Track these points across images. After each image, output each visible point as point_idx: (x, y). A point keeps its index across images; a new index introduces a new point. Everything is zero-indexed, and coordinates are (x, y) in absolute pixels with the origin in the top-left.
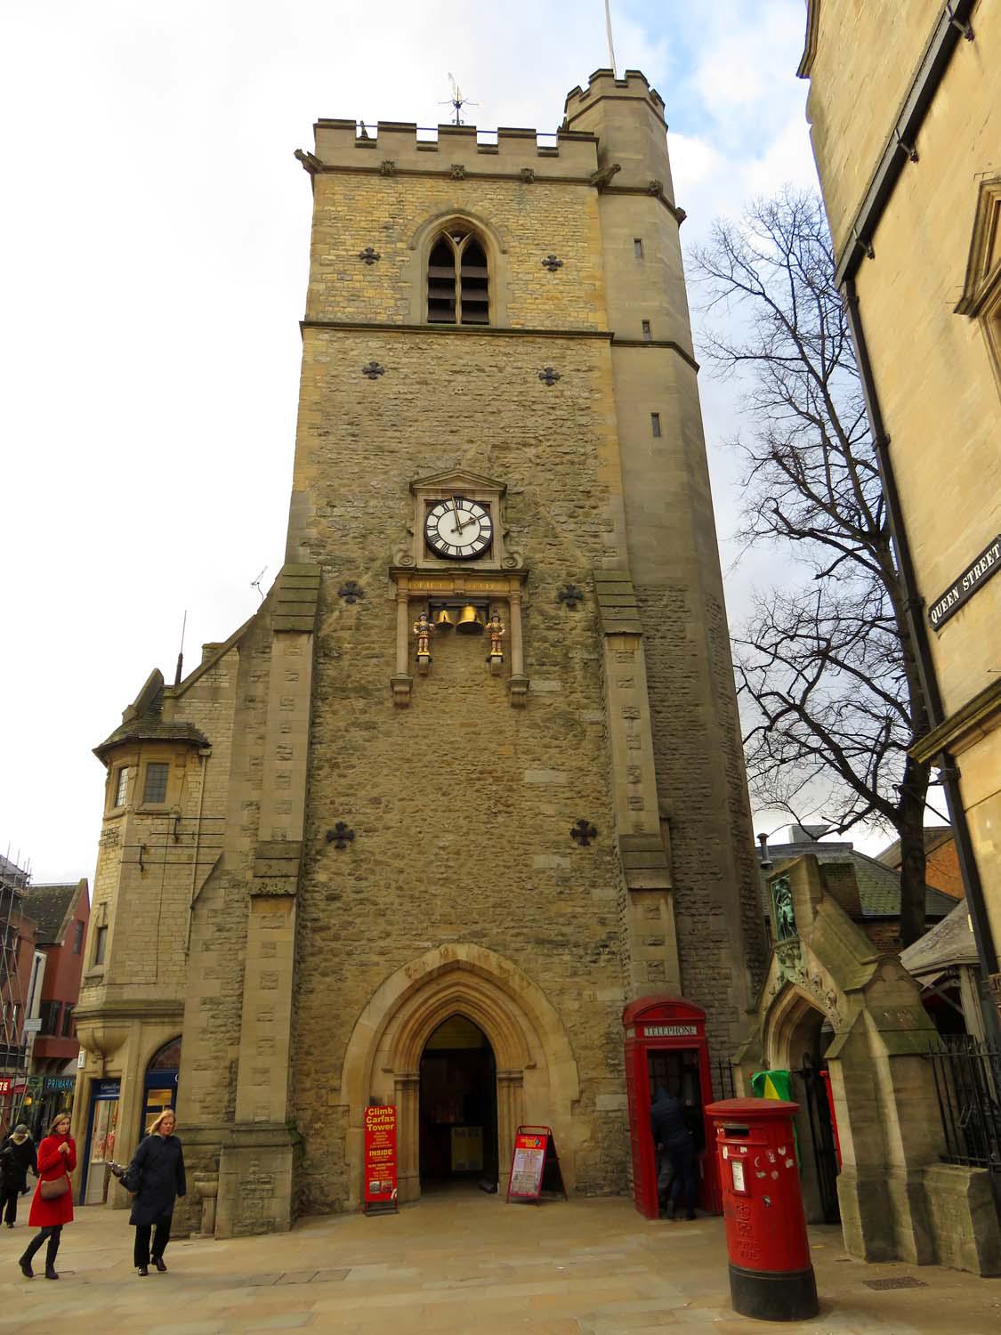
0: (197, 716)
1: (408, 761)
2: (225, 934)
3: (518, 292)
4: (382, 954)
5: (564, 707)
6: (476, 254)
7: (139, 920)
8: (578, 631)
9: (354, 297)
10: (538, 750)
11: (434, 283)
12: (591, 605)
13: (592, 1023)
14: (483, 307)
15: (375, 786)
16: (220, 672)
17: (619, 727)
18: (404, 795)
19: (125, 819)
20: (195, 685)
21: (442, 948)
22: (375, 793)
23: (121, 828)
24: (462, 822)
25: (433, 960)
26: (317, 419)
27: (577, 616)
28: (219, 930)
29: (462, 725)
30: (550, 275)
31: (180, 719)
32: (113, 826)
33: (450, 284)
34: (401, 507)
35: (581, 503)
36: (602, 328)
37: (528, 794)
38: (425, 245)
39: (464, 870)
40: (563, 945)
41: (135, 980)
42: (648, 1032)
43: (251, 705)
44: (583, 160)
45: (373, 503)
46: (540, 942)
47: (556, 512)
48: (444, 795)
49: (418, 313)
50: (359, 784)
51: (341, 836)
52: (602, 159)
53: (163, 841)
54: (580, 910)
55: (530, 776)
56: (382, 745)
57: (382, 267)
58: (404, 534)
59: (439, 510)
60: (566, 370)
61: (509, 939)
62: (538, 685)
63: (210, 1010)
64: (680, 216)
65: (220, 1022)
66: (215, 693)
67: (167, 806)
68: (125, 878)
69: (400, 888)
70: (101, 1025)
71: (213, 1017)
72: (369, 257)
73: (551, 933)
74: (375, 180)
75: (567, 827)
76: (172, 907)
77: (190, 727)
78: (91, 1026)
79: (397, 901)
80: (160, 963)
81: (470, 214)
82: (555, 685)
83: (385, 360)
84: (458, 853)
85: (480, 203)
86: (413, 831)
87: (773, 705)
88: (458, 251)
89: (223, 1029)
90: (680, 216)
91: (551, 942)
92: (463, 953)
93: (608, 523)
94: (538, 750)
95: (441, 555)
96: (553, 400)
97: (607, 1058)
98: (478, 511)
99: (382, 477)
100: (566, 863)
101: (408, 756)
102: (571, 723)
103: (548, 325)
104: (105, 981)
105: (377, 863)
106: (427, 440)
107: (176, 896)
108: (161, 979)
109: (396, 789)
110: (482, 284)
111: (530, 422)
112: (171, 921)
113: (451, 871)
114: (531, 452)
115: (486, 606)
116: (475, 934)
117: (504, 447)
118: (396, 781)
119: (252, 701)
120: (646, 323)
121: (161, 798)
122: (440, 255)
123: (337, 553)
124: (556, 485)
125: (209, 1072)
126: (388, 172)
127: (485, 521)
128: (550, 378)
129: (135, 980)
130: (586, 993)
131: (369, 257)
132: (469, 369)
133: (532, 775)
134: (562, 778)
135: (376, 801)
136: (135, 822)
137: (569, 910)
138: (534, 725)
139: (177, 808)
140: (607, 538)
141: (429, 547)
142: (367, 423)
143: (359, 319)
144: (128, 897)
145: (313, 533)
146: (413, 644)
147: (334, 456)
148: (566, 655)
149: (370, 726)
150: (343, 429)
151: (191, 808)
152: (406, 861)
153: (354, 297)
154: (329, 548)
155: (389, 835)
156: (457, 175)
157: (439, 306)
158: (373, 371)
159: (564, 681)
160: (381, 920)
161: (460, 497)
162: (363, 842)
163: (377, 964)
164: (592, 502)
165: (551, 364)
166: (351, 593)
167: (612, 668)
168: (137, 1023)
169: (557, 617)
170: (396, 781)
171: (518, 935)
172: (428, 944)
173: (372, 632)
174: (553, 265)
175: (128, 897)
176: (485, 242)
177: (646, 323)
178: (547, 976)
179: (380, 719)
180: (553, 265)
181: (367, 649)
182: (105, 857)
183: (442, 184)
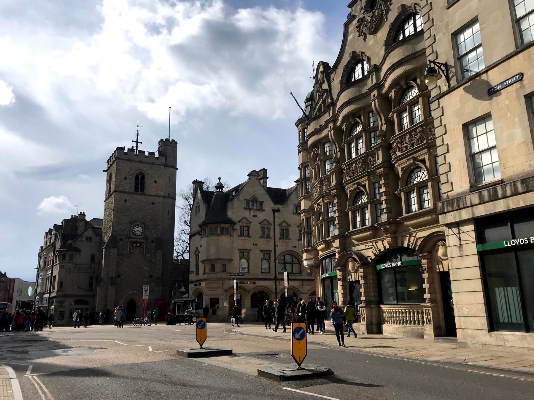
3: (150, 187)
6: (143, 177)
11: (136, 184)
25: (130, 293)
26: (116, 209)
38: (135, 175)
51: (119, 276)
57: (127, 180)
62: (147, 255)
64: (177, 169)
66: (82, 241)
72: (126, 178)
74: (127, 162)
77: (77, 248)
85: (145, 168)
87: (179, 254)
88: (140, 177)
90: (177, 169)
92: (134, 292)
95: (135, 235)
110: (143, 184)
115: (140, 243)
122: (137, 177)
126: (129, 160)
128: (153, 204)
131: (126, 178)
145: (116, 229)
146: (130, 248)
156: (141, 162)
157: (136, 188)
158: (125, 201)
162: (122, 277)
166: (121, 240)
180: (156, 182)
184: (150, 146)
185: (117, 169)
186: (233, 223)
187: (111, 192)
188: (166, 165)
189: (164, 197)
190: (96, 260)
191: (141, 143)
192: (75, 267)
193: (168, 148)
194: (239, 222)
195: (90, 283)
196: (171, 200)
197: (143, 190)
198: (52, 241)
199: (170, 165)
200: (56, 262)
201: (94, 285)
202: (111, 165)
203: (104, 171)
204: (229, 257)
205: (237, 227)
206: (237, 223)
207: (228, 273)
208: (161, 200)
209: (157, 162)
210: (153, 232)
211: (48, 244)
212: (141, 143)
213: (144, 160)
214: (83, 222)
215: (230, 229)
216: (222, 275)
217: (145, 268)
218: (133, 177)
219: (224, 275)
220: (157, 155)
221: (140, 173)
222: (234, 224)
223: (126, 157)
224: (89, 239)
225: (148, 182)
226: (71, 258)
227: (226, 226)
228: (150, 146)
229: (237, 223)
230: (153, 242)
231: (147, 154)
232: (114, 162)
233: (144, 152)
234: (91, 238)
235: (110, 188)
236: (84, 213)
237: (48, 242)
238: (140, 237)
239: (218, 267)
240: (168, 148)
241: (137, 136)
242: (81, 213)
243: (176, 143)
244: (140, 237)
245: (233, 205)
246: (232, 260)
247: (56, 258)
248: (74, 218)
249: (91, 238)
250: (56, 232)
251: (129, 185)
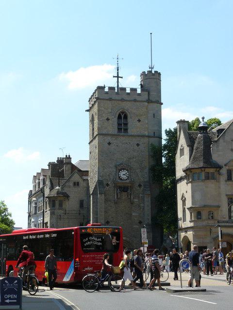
3: (134, 127)
6: (126, 117)
11: (119, 124)
33: (121, 124)
34: (115, 170)
36: (147, 134)
44: (145, 96)
49: (116, 131)
52: (149, 94)
55: (133, 214)
60: (141, 143)
64: (162, 104)
72: (108, 119)
74: (108, 102)
82: (137, 200)
83: (111, 142)
85: (127, 106)
88: (123, 116)
90: (162, 104)
93: (146, 173)
95: (121, 179)
98: (127, 172)
110: (126, 124)
114: (134, 160)
120: (154, 133)
122: (119, 117)
126: (110, 99)
127: (128, 174)
128: (138, 145)
131: (108, 119)
134: (138, 214)
141: (119, 177)
156: (122, 100)
157: (119, 130)
158: (109, 144)
161: (124, 169)
167: (146, 199)
174: (139, 121)
177: (154, 133)
180: (139, 121)
183: (120, 102)
184: (132, 81)
185: (99, 110)
186: (219, 167)
187: (95, 136)
188: (149, 101)
189: (149, 137)
191: (122, 78)
192: (65, 214)
193: (152, 79)
194: (225, 165)
196: (157, 139)
197: (126, 130)
198: (41, 186)
199: (154, 100)
200: (46, 209)
202: (93, 105)
203: (86, 111)
204: (216, 204)
205: (224, 171)
206: (224, 167)
207: (216, 220)
208: (146, 139)
209: (138, 98)
211: (37, 189)
212: (122, 78)
213: (126, 97)
214: (69, 166)
215: (216, 175)
216: (209, 222)
218: (115, 117)
219: (211, 222)
220: (139, 91)
221: (123, 113)
222: (220, 167)
223: (107, 97)
224: (76, 184)
225: (132, 123)
226: (61, 205)
227: (212, 170)
228: (132, 81)
229: (224, 167)
230: (140, 186)
231: (128, 91)
232: (95, 102)
233: (124, 89)
235: (93, 129)
236: (69, 156)
237: (37, 187)
238: (128, 181)
239: (204, 215)
240: (152, 79)
241: (118, 70)
242: (66, 156)
243: (159, 74)
244: (128, 181)
245: (218, 147)
246: (219, 207)
247: (46, 203)
248: (60, 161)
250: (44, 177)
251: (112, 127)
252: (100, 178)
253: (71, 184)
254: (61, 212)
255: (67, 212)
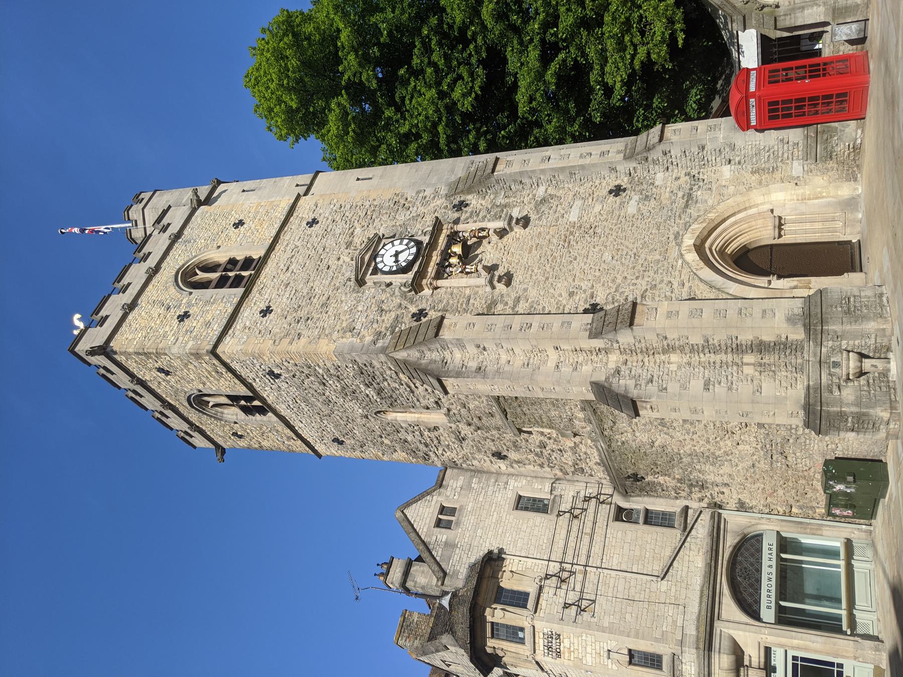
0: (464, 560)
1: (547, 278)
2: (655, 378)
4: (683, 285)
5: (532, 206)
7: (628, 616)
8: (483, 202)
9: (208, 324)
10: (557, 215)
11: (221, 283)
12: (469, 197)
13: (744, 180)
14: (248, 263)
15: (561, 295)
16: (433, 541)
17: (554, 163)
18: (571, 280)
19: (538, 625)
20: (438, 559)
21: (683, 252)
22: (565, 295)
23: (545, 631)
24: (597, 249)
27: (474, 202)
28: (652, 382)
29: (530, 252)
30: (245, 226)
31: (463, 572)
32: (541, 641)
35: (401, 205)
37: (585, 218)
39: (631, 246)
40: (690, 195)
41: (679, 623)
42: (752, 88)
43: (483, 368)
45: (360, 308)
46: (687, 206)
47: (402, 217)
48: (575, 259)
50: (557, 304)
53: (561, 593)
54: (668, 189)
56: (533, 293)
58: (388, 289)
59: (380, 266)
61: (682, 221)
63: (714, 385)
65: (724, 380)
67: (532, 590)
68: (589, 626)
69: (637, 278)
70: (717, 656)
71: (720, 383)
73: (681, 202)
75: (611, 198)
76: (621, 588)
77: (472, 567)
78: (717, 671)
79: (646, 279)
80: (668, 601)
81: (183, 265)
83: (263, 306)
84: (618, 250)
86: (597, 274)
89: (729, 378)
91: (687, 201)
92: (689, 241)
93: (418, 192)
94: (557, 215)
96: (329, 221)
97: (768, 173)
99: (344, 304)
100: (636, 197)
101: (544, 279)
102: (544, 201)
103: (277, 226)
104: (678, 652)
105: (616, 291)
106: (327, 282)
107: (611, 585)
108: (681, 602)
109: (566, 284)
110: (233, 262)
111: (338, 231)
112: (633, 590)
113: (630, 253)
114: (358, 230)
116: (676, 238)
117: (349, 245)
118: (559, 285)
119: (480, 368)
121: (527, 595)
123: (388, 326)
124: (385, 218)
125: (764, 385)
128: (313, 223)
129: (679, 623)
130: (724, 183)
132: (289, 262)
133: (573, 217)
135: (571, 294)
136: (542, 615)
137: (667, 194)
138: (540, 219)
139: (537, 580)
140: (429, 192)
142: (302, 313)
143: (225, 321)
144: (606, 624)
147: (318, 330)
148: (497, 206)
149: (518, 300)
150: (301, 326)
151: (540, 568)
152: (618, 276)
153: (208, 324)
154: (383, 330)
155: (598, 286)
157: (237, 282)
159: (514, 206)
160: (659, 286)
163: (690, 287)
164: (402, 201)
165: (304, 223)
168: (717, 624)
169: (472, 213)
170: (559, 285)
171: (680, 216)
172: (680, 262)
173: (451, 302)
174: (239, 224)
175: (606, 624)
176: (206, 260)
178: (710, 203)
179: (513, 295)
180: (239, 224)
181: (462, 304)
182: (567, 655)
190: (540, 490)
195: (647, 522)
201: (658, 505)
210: (422, 210)
217: (573, 217)
234: (443, 510)
249: (443, 510)
252: (380, 344)
253: (443, 535)
254: (552, 600)
255: (554, 568)
